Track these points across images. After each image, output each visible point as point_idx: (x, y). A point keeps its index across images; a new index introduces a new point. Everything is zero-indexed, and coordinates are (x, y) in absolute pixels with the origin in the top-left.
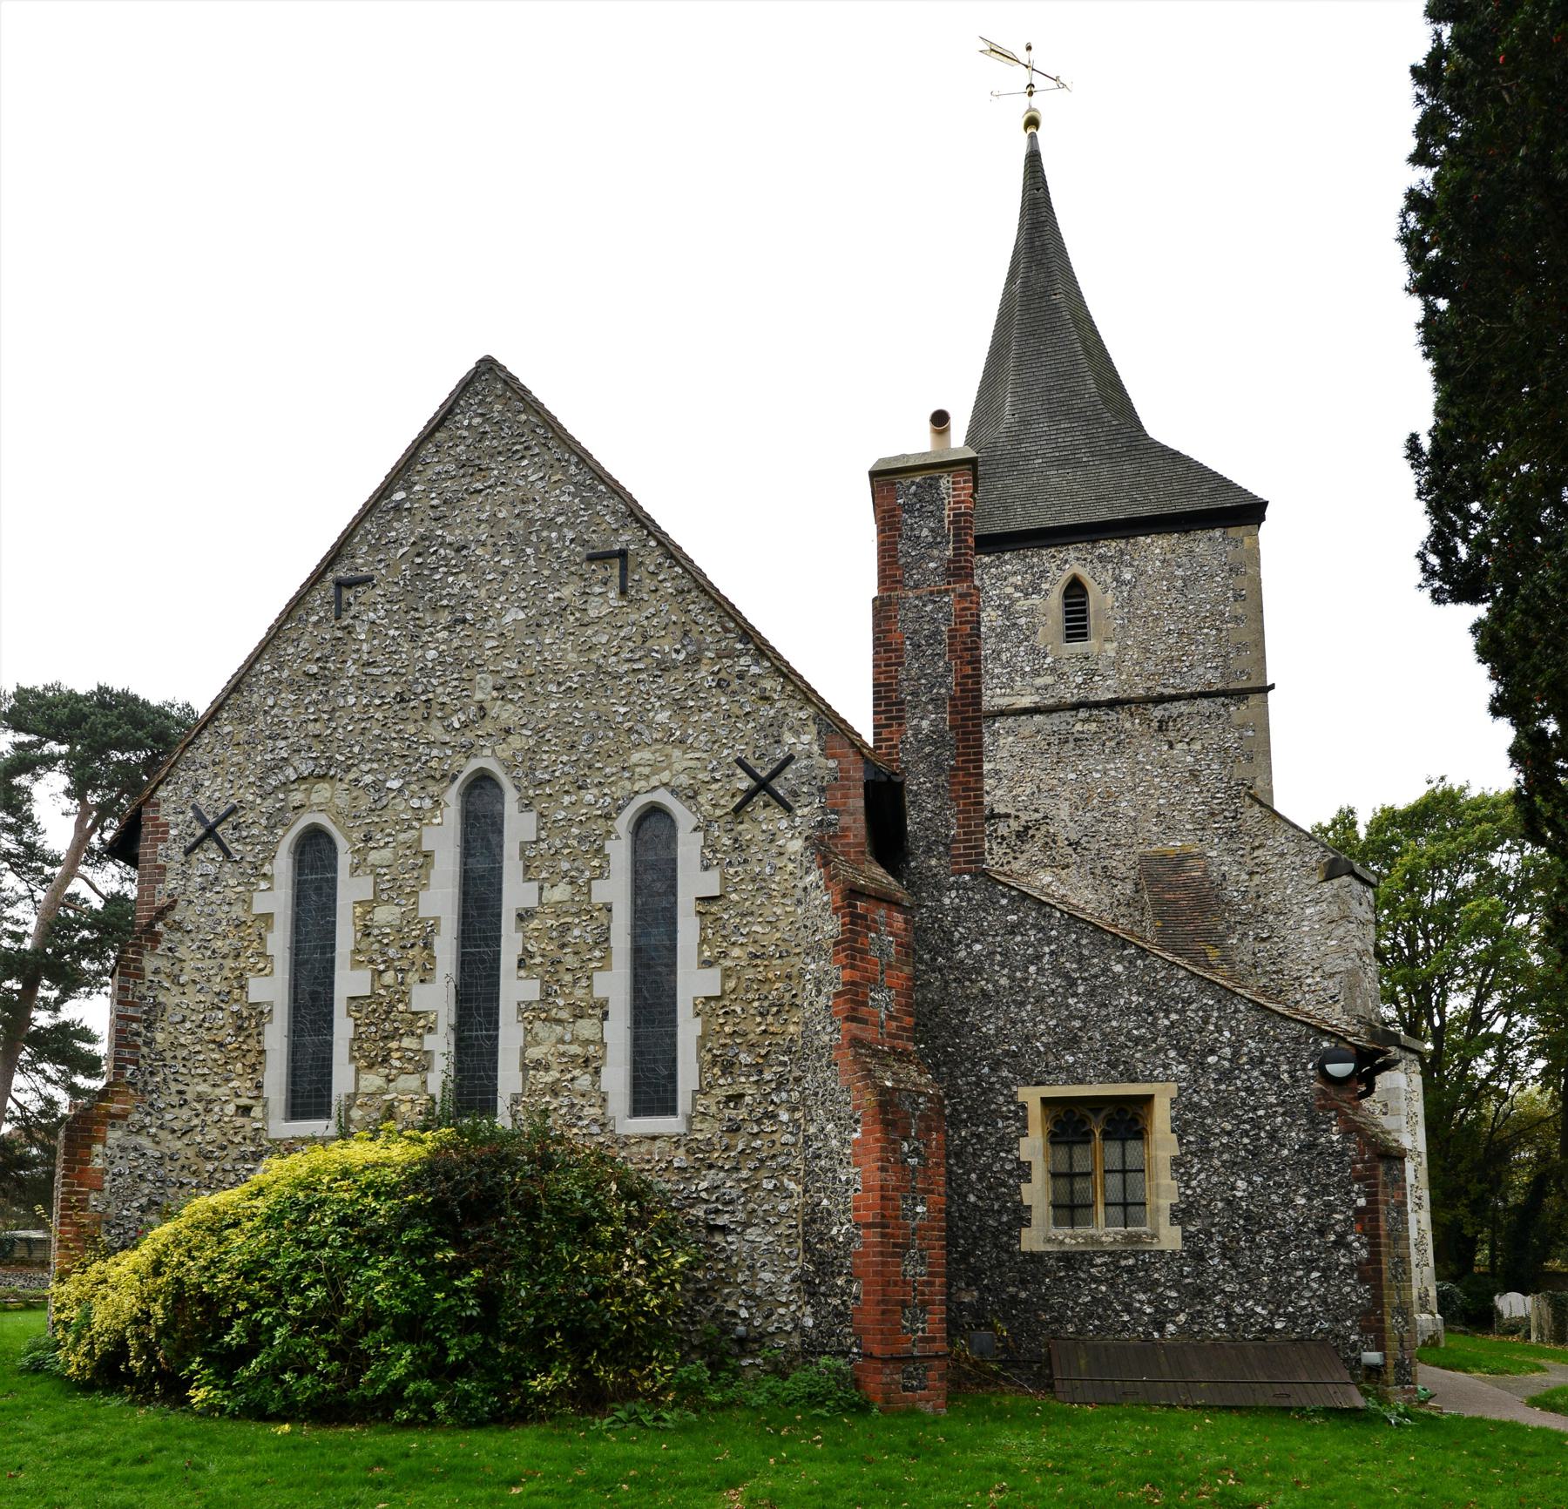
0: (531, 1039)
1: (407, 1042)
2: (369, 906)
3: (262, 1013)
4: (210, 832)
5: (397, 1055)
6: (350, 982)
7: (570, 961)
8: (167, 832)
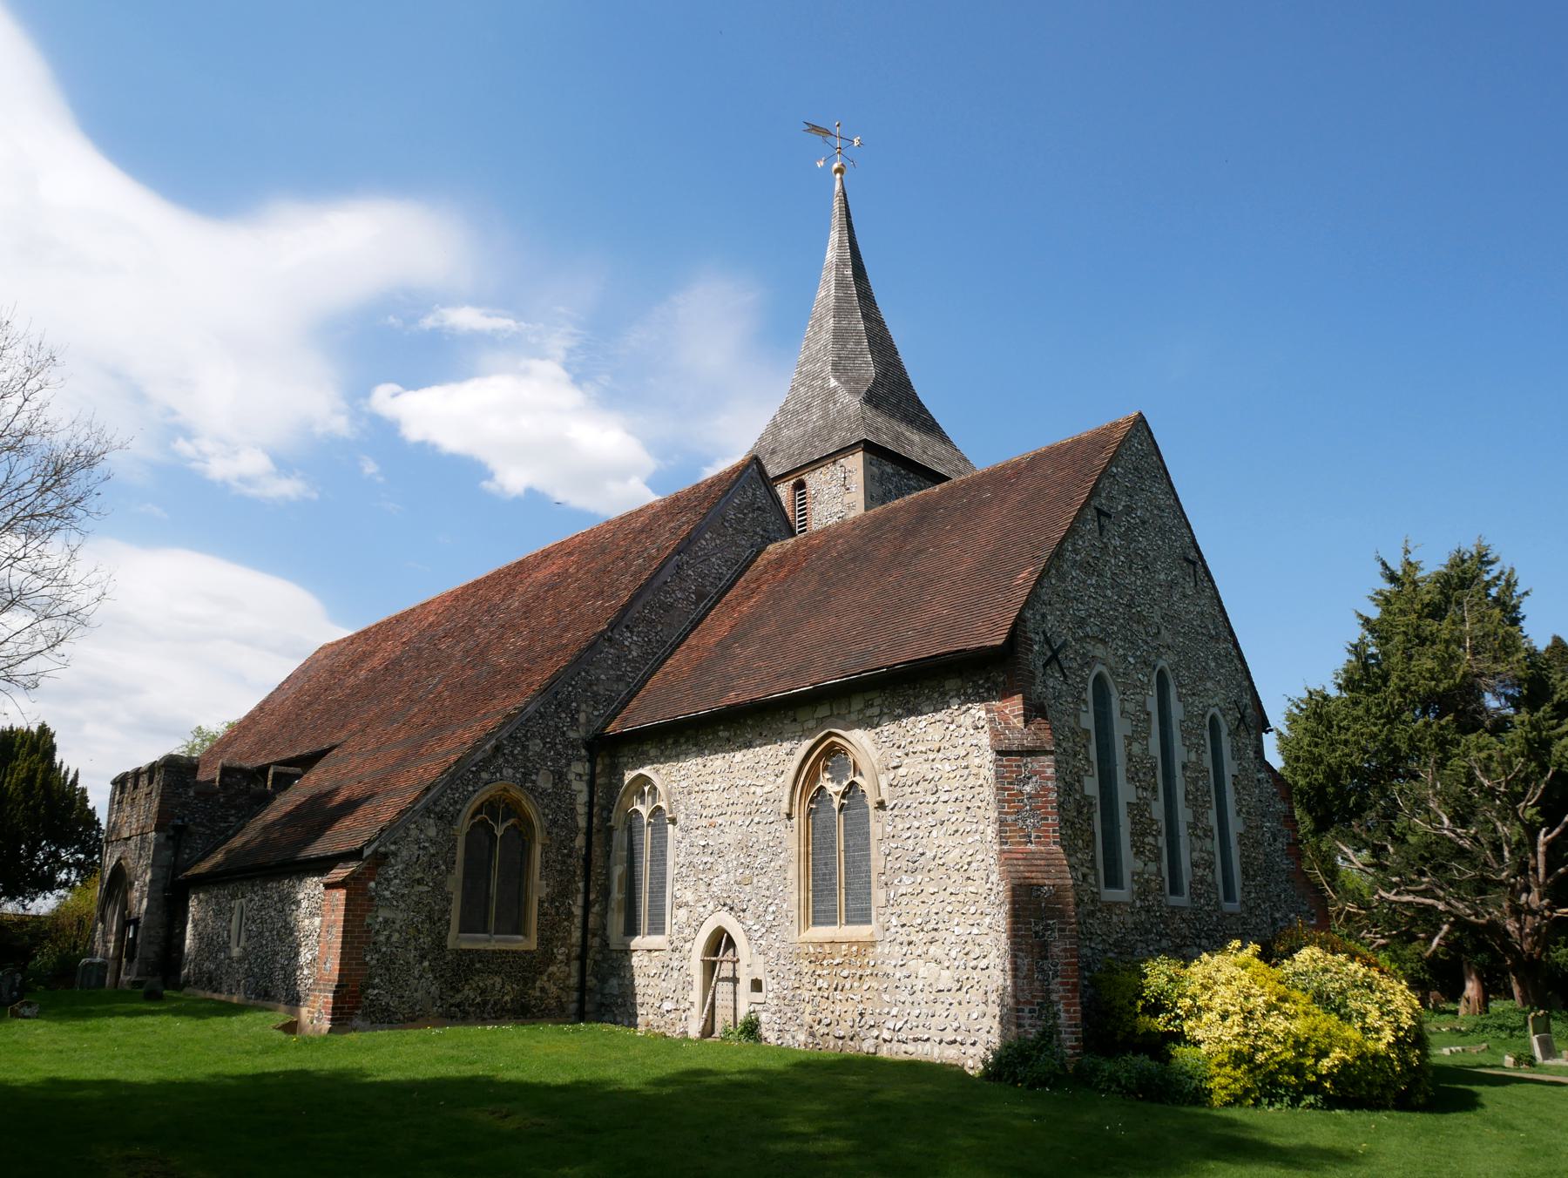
2: (1130, 740)
3: (1091, 804)
4: (1054, 657)
5: (1148, 847)
6: (1126, 793)
8: (1032, 646)
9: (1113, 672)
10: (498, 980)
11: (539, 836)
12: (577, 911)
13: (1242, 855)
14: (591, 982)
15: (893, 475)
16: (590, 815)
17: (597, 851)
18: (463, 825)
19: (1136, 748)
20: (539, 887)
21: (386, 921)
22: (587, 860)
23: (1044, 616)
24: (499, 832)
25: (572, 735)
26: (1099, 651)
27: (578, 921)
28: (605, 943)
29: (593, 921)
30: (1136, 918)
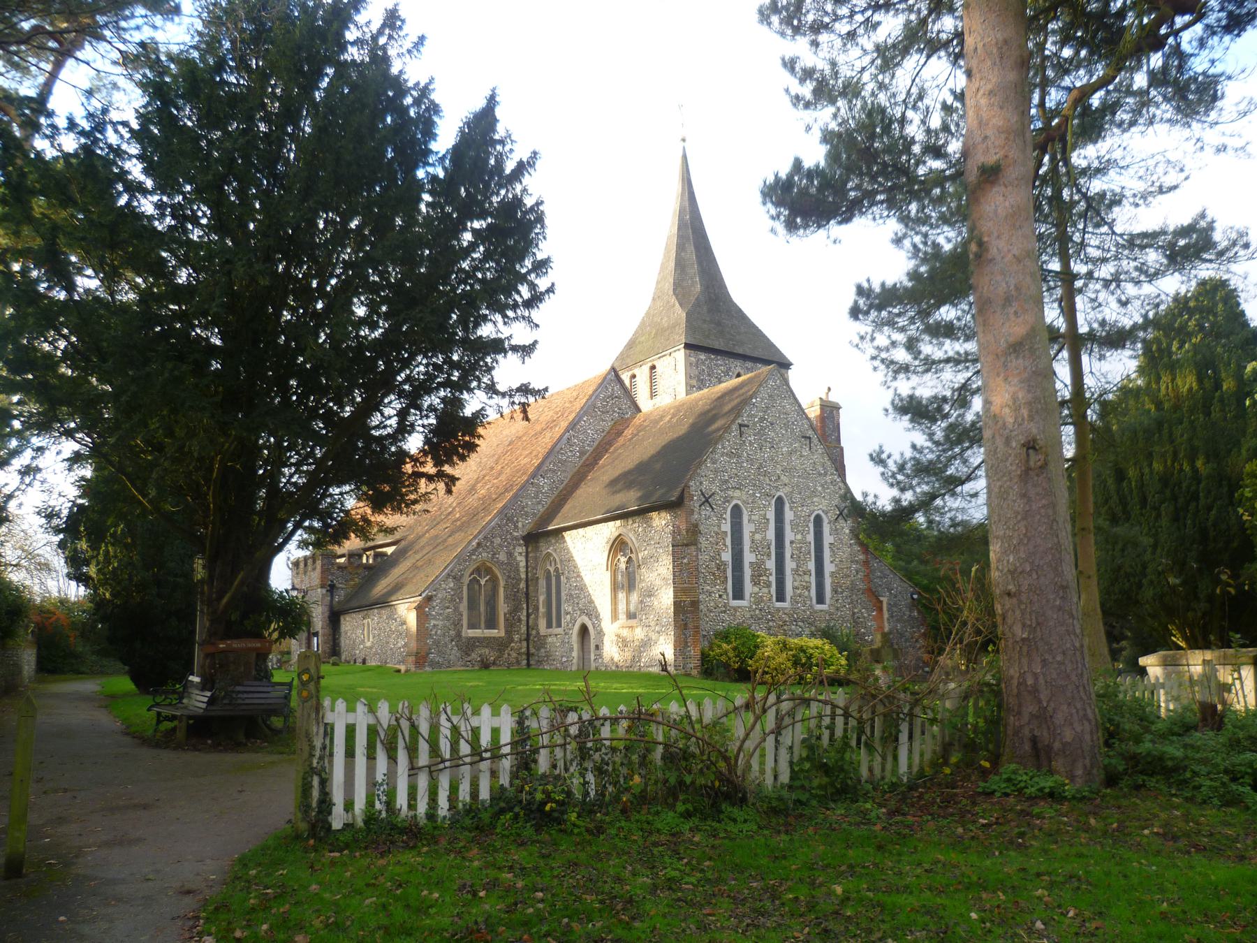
0: (795, 580)
1: (765, 578)
2: (753, 533)
6: (749, 557)
7: (802, 557)
9: (744, 502)
10: (487, 651)
11: (502, 583)
12: (524, 618)
13: (833, 582)
14: (532, 650)
15: (706, 360)
16: (527, 572)
17: (531, 588)
18: (466, 580)
19: (758, 537)
20: (503, 608)
21: (434, 625)
22: (527, 594)
23: (701, 483)
24: (483, 582)
25: (516, 534)
26: (737, 493)
27: (524, 623)
28: (538, 633)
29: (531, 622)
30: (752, 613)
